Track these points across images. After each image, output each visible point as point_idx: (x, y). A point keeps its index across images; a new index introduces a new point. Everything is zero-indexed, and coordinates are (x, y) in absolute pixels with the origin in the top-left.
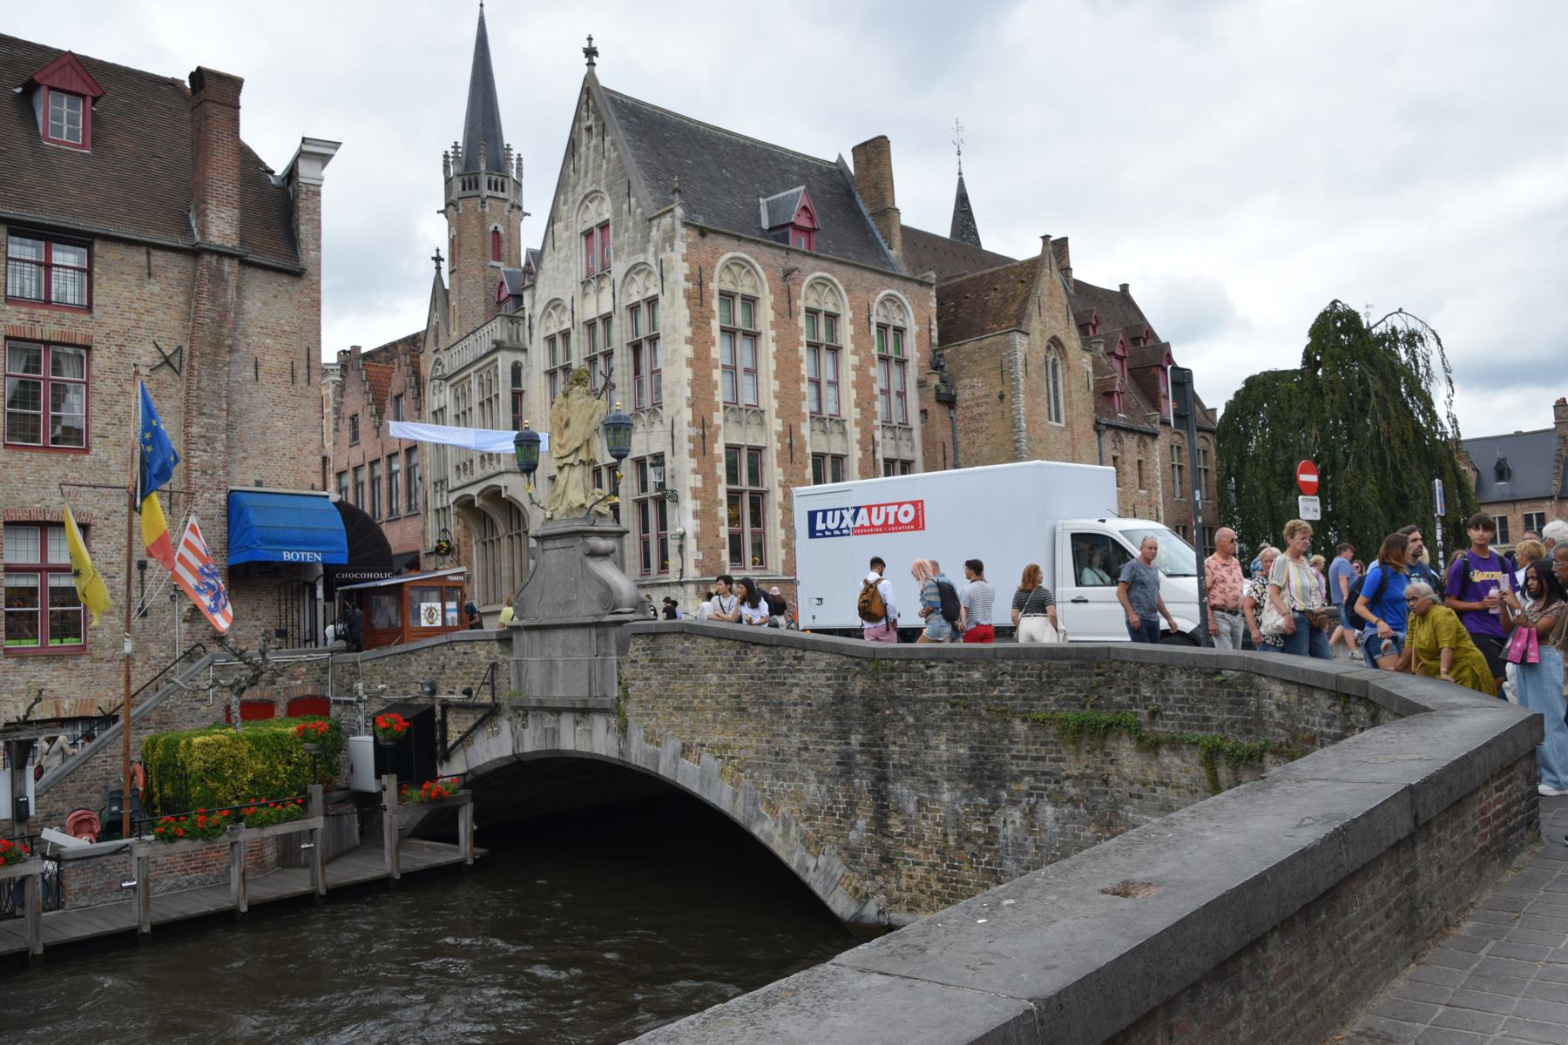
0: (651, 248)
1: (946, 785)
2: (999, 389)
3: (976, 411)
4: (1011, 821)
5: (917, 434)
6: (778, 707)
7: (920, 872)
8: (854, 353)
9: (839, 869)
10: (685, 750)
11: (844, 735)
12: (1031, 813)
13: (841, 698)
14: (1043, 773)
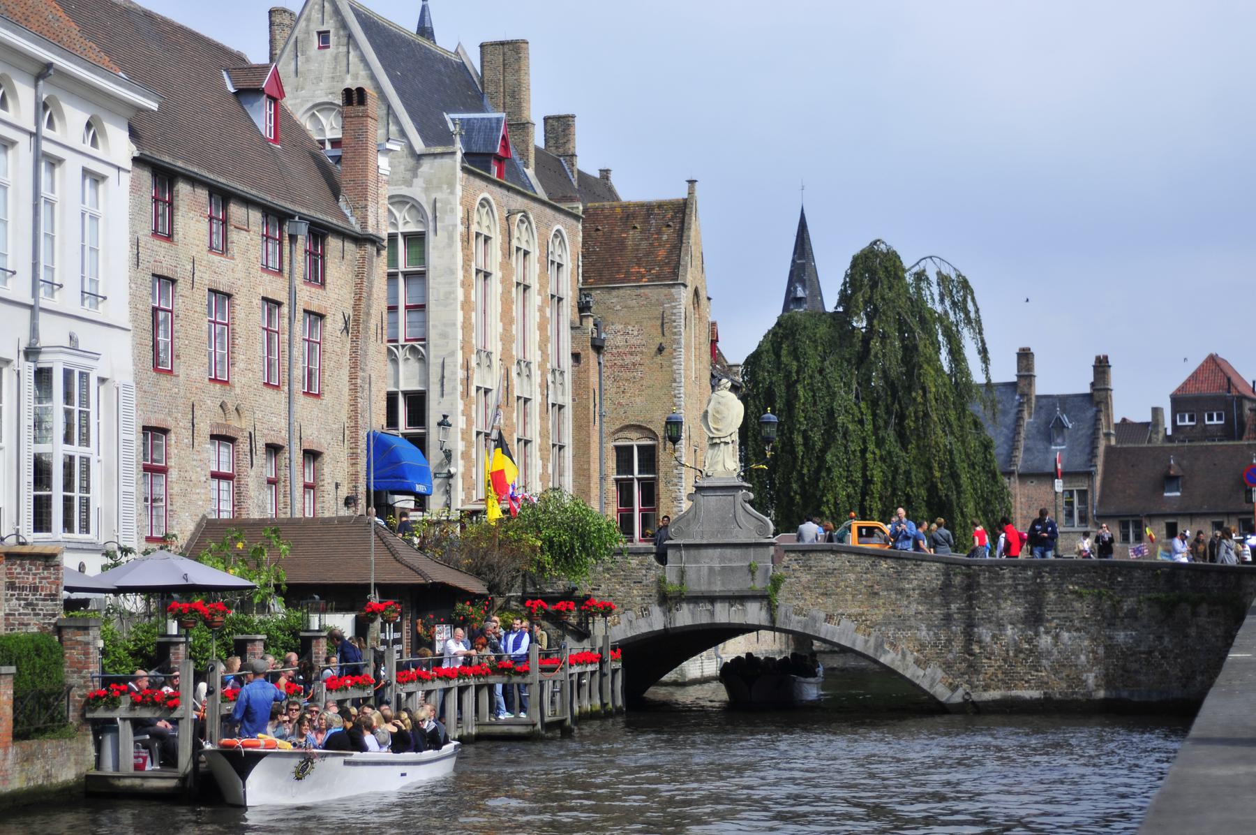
0: (419, 182)
1: (1010, 627)
2: (659, 340)
3: (628, 360)
4: (1045, 641)
5: (568, 377)
6: (900, 591)
7: (992, 670)
8: (539, 294)
9: (940, 674)
10: (829, 618)
11: (946, 604)
12: (1057, 637)
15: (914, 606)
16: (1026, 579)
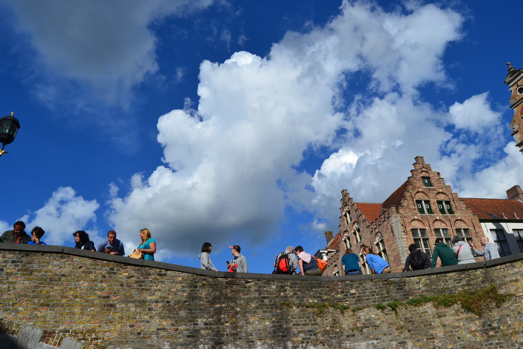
1: (259, 343)
11: (193, 320)
13: (192, 297)
14: (308, 331)
15: (156, 322)
16: (270, 293)
